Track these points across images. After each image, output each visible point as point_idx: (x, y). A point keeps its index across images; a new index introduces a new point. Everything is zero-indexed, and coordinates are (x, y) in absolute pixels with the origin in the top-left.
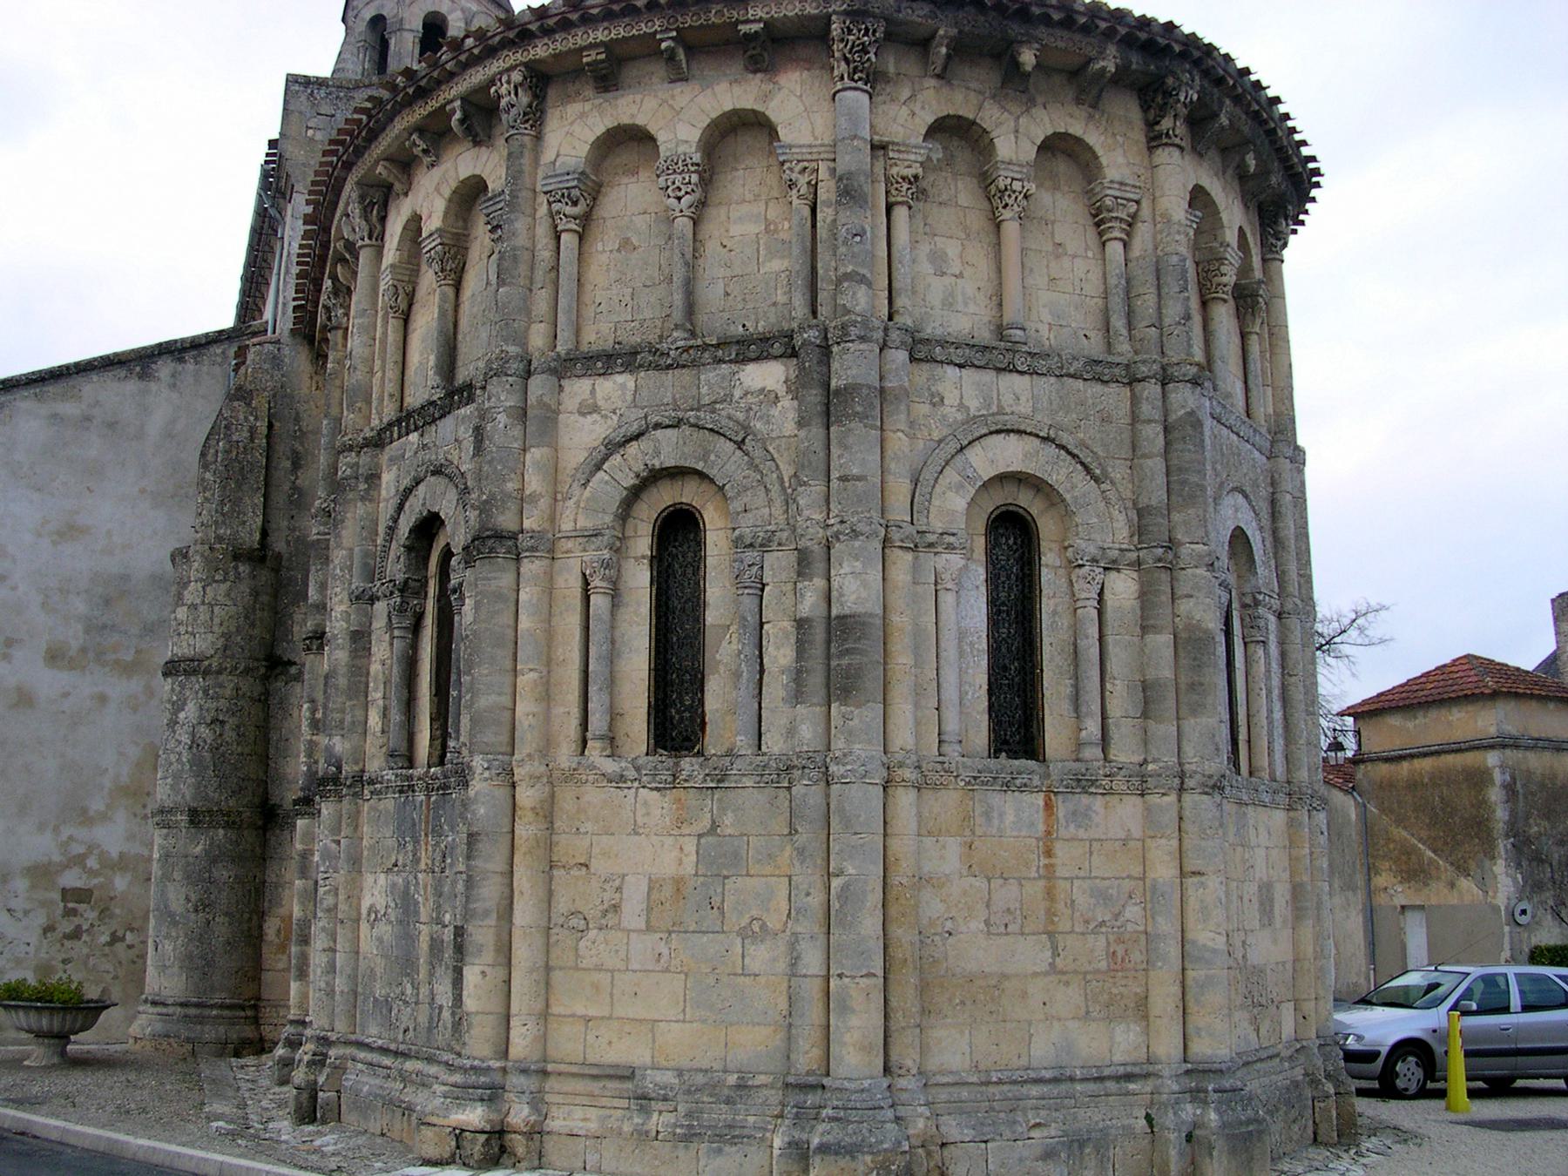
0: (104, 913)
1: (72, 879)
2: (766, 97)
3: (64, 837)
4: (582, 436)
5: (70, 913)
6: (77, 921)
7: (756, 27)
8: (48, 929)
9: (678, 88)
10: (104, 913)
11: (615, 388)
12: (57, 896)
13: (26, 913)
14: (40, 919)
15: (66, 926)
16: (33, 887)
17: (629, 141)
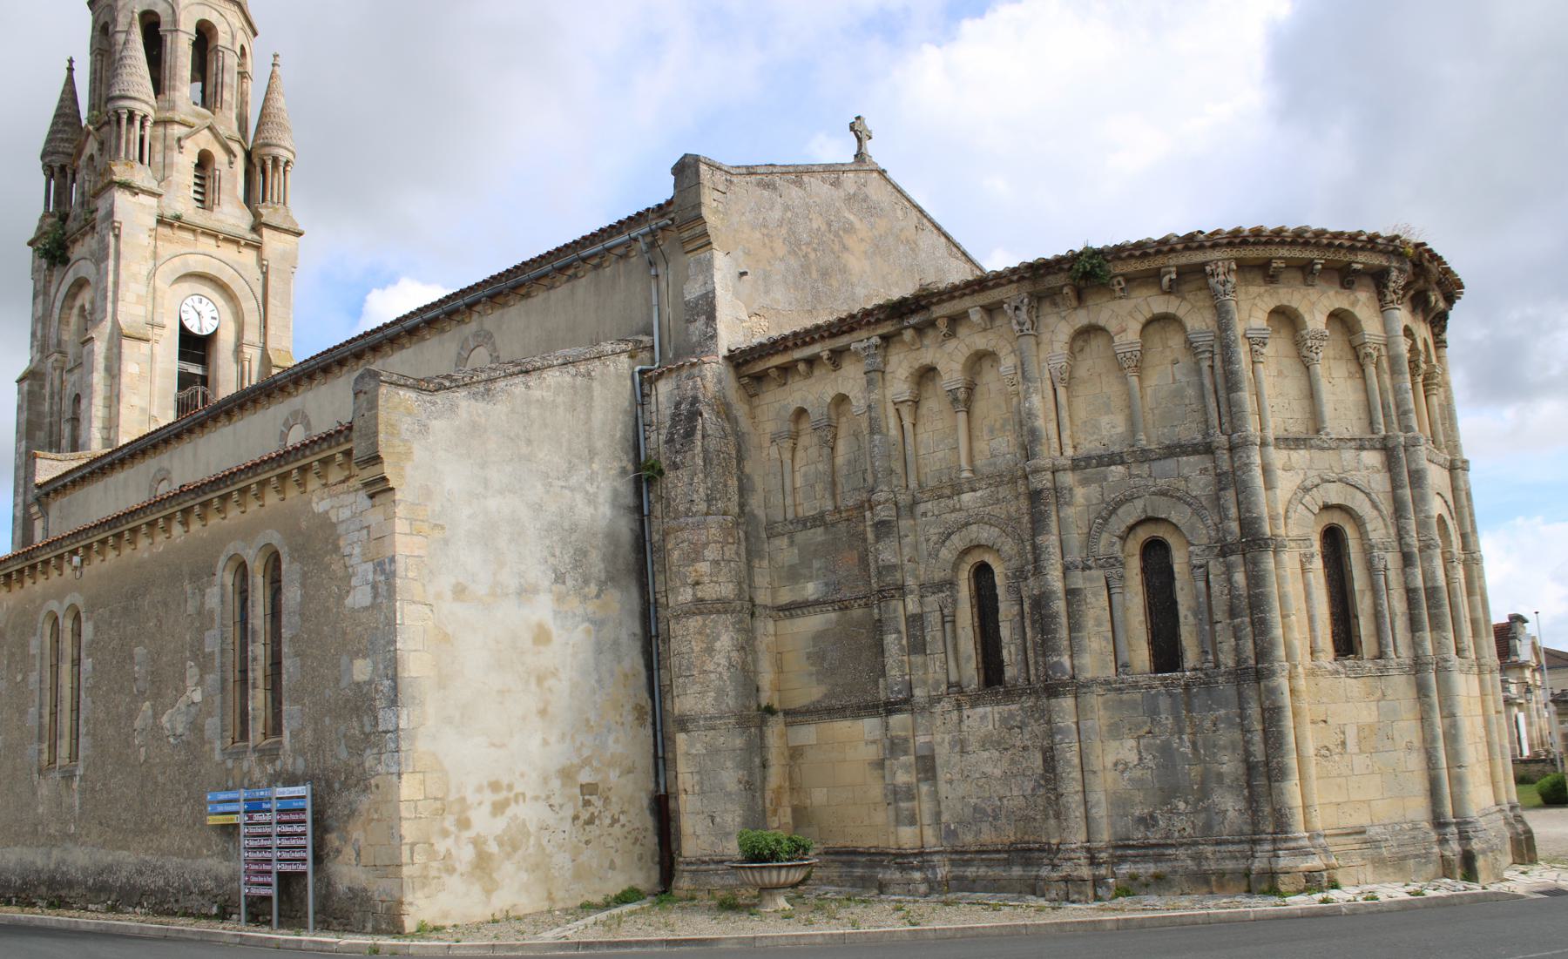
0: (607, 800)
1: (585, 777)
2: (1353, 304)
3: (578, 744)
4: (1286, 484)
5: (587, 803)
6: (591, 809)
7: (1359, 266)
8: (576, 818)
9: (1311, 290)
10: (607, 800)
11: (1300, 456)
12: (578, 791)
13: (561, 806)
14: (569, 812)
15: (585, 815)
16: (563, 785)
17: (1285, 317)
